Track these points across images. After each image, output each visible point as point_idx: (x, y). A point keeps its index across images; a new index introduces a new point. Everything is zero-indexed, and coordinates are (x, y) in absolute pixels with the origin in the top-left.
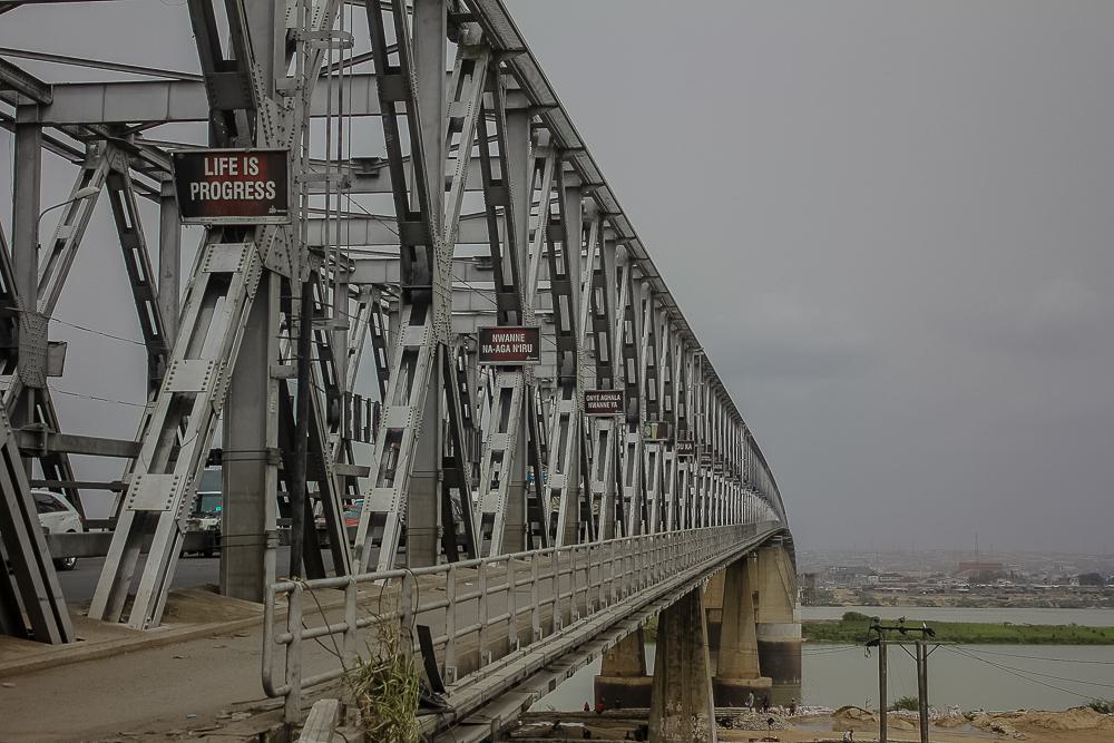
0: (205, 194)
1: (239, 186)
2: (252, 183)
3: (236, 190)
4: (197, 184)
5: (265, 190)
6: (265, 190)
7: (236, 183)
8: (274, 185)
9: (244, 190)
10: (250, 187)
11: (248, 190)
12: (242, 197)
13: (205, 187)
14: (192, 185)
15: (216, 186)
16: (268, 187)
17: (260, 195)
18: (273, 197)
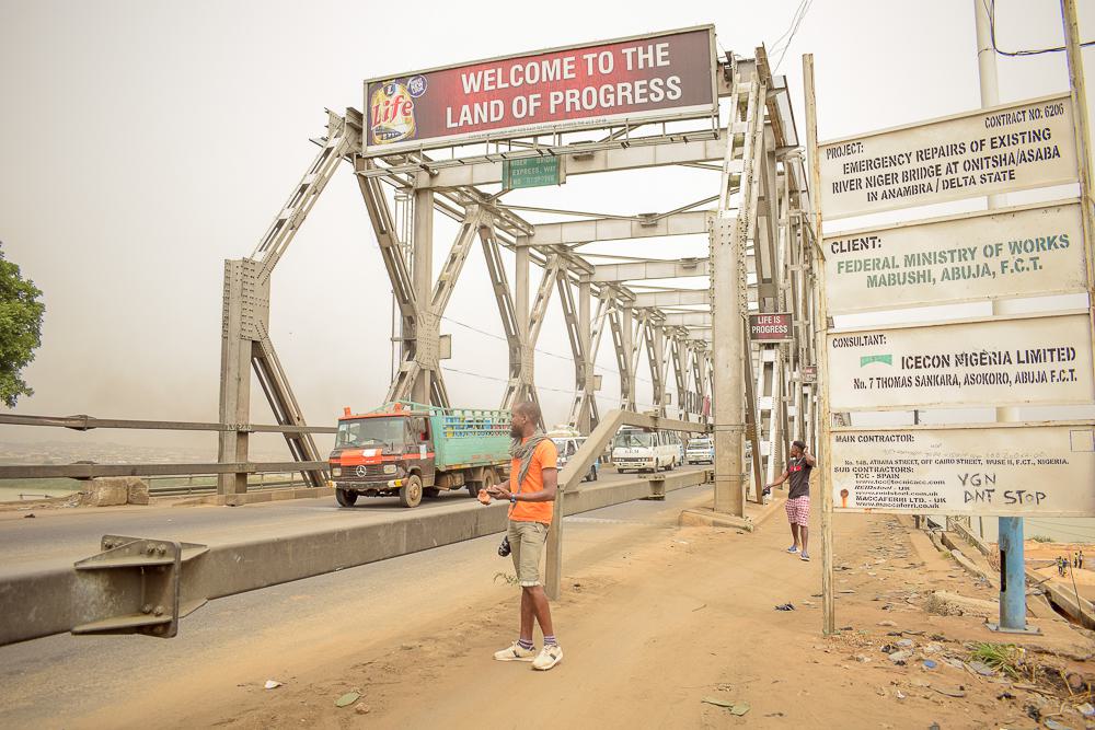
0: (573, 104)
1: (624, 89)
2: (645, 82)
3: (620, 94)
4: (560, 94)
5: (665, 88)
6: (665, 88)
7: (620, 86)
8: (678, 80)
9: (633, 93)
10: (641, 87)
11: (638, 91)
12: (630, 101)
13: (572, 95)
14: (552, 95)
15: (589, 93)
17: (657, 95)
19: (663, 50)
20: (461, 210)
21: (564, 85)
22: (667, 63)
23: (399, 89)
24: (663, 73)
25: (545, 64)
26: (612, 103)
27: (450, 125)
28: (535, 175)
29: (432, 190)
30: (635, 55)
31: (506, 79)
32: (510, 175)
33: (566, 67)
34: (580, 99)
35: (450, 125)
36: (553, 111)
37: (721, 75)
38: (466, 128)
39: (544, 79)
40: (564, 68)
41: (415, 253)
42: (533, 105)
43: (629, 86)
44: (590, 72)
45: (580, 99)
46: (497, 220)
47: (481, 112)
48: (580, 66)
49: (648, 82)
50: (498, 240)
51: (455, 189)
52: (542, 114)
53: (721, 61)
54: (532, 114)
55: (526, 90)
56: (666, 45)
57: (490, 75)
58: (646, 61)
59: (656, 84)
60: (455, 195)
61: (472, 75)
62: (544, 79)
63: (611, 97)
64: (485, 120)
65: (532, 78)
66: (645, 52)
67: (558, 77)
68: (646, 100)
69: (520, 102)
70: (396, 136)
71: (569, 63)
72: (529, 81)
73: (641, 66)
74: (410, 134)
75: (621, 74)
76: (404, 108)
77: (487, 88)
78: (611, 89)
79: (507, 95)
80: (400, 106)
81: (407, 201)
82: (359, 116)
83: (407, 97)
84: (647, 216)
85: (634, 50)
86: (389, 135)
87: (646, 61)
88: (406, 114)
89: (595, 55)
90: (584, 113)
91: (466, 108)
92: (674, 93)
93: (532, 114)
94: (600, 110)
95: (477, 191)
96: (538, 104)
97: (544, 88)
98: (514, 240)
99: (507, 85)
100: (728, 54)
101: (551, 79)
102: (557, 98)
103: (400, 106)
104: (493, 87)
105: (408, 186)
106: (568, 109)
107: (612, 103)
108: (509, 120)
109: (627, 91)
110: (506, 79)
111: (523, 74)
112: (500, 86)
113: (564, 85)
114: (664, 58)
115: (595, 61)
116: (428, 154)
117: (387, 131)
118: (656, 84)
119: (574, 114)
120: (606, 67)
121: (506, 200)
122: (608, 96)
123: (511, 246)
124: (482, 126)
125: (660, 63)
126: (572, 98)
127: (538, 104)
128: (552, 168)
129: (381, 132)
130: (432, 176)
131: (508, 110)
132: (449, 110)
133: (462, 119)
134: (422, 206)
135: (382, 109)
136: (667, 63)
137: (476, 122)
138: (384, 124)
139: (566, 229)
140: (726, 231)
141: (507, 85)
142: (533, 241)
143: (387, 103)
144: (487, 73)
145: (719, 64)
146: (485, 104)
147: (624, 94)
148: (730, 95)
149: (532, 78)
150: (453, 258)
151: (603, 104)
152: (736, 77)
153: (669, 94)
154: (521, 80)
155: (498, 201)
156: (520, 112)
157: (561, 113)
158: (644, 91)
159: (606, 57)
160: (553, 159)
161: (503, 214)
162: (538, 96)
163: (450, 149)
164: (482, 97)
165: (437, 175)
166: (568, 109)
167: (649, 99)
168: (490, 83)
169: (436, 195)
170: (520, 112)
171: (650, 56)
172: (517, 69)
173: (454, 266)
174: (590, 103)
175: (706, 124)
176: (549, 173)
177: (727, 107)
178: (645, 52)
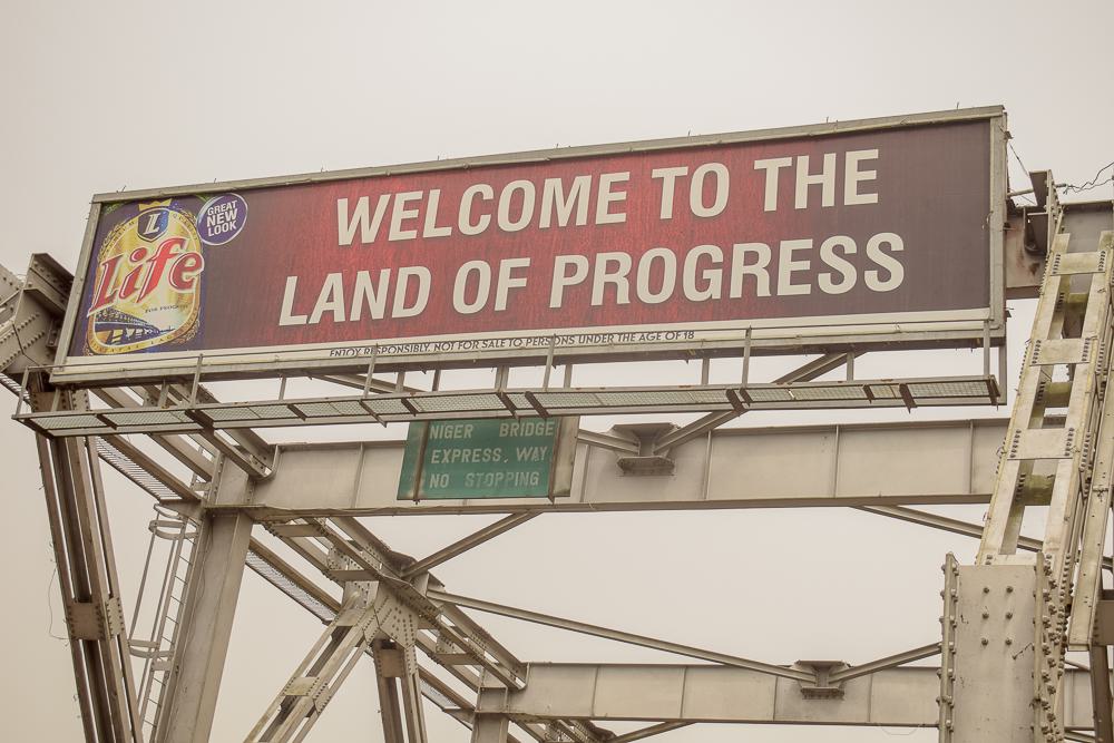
0: (611, 288)
2: (807, 244)
3: (739, 270)
4: (581, 262)
5: (861, 262)
6: (861, 262)
7: (739, 250)
8: (897, 243)
9: (773, 269)
10: (797, 255)
11: (787, 266)
12: (763, 290)
13: (613, 267)
14: (561, 262)
15: (658, 264)
16: (873, 251)
17: (837, 278)
18: (897, 280)
19: (863, 165)
20: (335, 591)
21: (592, 239)
22: (872, 198)
23: (176, 222)
24: (859, 223)
25: (553, 185)
26: (715, 292)
27: (286, 319)
28: (491, 467)
29: (249, 515)
30: (787, 176)
31: (447, 215)
32: (424, 461)
33: (605, 196)
34: (632, 277)
35: (286, 319)
36: (556, 301)
37: (1018, 241)
38: (328, 330)
39: (545, 222)
40: (599, 197)
41: (176, 675)
42: (506, 283)
43: (764, 251)
44: (666, 212)
45: (632, 277)
46: (430, 636)
47: (372, 294)
48: (642, 196)
49: (817, 246)
50: (423, 686)
51: (313, 521)
52: (527, 308)
53: (1019, 202)
54: (501, 305)
55: (493, 246)
56: (873, 154)
57: (408, 205)
58: (814, 191)
59: (838, 250)
60: (320, 546)
61: (364, 202)
62: (545, 222)
63: (715, 276)
64: (377, 312)
65: (515, 215)
66: (816, 169)
67: (581, 220)
68: (805, 289)
69: (474, 276)
70: (144, 337)
71: (615, 187)
72: (504, 224)
73: (801, 202)
74: (181, 333)
75: (745, 222)
76: (180, 268)
77: (396, 234)
78: (717, 254)
79: (444, 257)
80: (170, 264)
81: (183, 536)
82: (63, 280)
83: (193, 244)
84: (820, 668)
85: (787, 162)
86: (124, 330)
87: (814, 191)
88: (179, 283)
89: (683, 171)
90: (638, 312)
91: (334, 280)
92: (884, 275)
93: (501, 305)
94: (679, 308)
95: (379, 547)
96: (522, 282)
97: (541, 245)
98: (471, 697)
99: (447, 231)
100: (1040, 181)
101: (563, 222)
102: (571, 270)
103: (170, 264)
104: (411, 234)
105: (188, 500)
106: (597, 299)
107: (715, 292)
108: (440, 317)
109: (751, 263)
110: (447, 215)
111: (491, 207)
112: (431, 231)
113: (592, 239)
114: (863, 187)
115: (683, 185)
116: (208, 386)
117: (126, 321)
118: (838, 250)
119: (612, 312)
120: (708, 200)
121: (454, 578)
122: (707, 274)
123: (463, 711)
124: (367, 327)
125: (852, 198)
126: (609, 274)
127: (522, 282)
128: (537, 453)
129: (108, 324)
130: (256, 481)
131: (442, 291)
132: (292, 282)
133: (321, 306)
134: (217, 556)
135: (124, 269)
136: (872, 198)
137: (356, 316)
138: (121, 305)
139: (608, 685)
140: (997, 605)
141: (447, 231)
142: (521, 706)
143: (141, 254)
144: (401, 198)
145: (1013, 211)
146: (385, 274)
147: (750, 269)
148: (1033, 292)
149: (515, 215)
150: (287, 706)
151: (692, 294)
152: (1058, 241)
153: (871, 278)
154: (485, 220)
155: (433, 581)
156: (470, 297)
157: (578, 307)
158: (805, 265)
159: (711, 179)
160: (541, 428)
161: (446, 621)
162: (525, 262)
163: (278, 381)
164: (380, 255)
165: (270, 479)
166: (597, 299)
167: (815, 287)
168: (406, 225)
169: (259, 533)
170: (470, 297)
171: (827, 179)
172: (478, 195)
173: (283, 728)
174: (655, 287)
175: (967, 363)
176: (528, 465)
177: (1027, 319)
178: (816, 169)
